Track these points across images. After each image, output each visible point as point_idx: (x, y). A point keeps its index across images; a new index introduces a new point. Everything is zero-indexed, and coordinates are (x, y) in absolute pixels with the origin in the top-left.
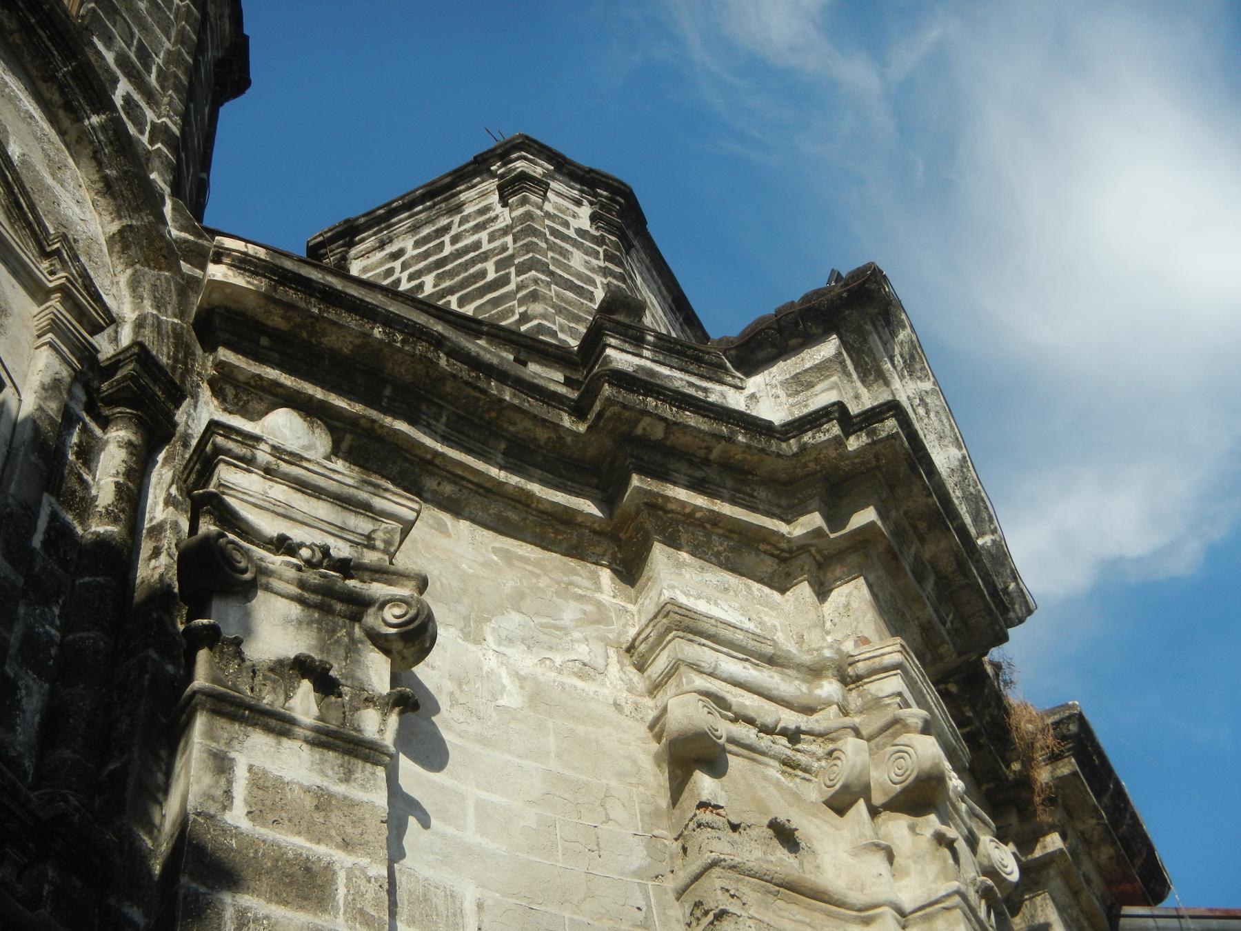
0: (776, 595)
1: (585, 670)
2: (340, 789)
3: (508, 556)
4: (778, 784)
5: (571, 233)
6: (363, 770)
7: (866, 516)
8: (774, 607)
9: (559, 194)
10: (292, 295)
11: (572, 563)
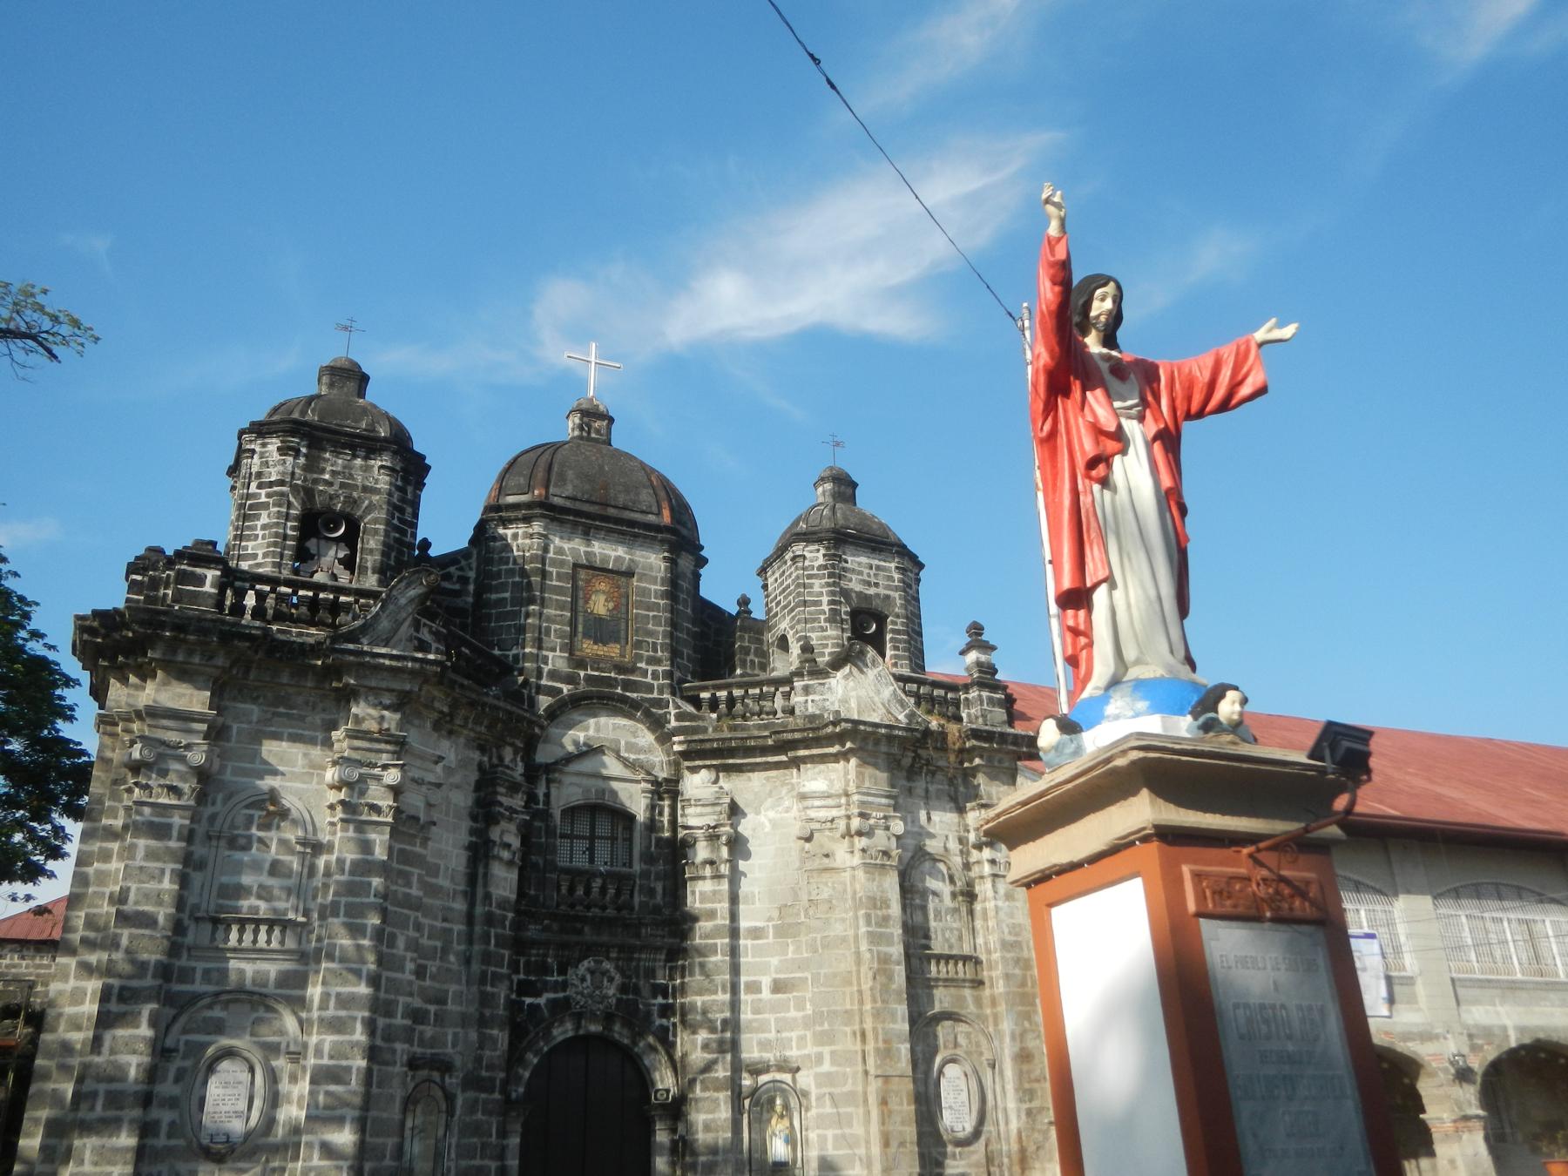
0: (837, 765)
2: (717, 888)
3: (767, 779)
4: (828, 837)
5: (815, 572)
6: (722, 880)
7: (849, 745)
8: (834, 770)
9: (811, 552)
10: (693, 745)
11: (786, 771)
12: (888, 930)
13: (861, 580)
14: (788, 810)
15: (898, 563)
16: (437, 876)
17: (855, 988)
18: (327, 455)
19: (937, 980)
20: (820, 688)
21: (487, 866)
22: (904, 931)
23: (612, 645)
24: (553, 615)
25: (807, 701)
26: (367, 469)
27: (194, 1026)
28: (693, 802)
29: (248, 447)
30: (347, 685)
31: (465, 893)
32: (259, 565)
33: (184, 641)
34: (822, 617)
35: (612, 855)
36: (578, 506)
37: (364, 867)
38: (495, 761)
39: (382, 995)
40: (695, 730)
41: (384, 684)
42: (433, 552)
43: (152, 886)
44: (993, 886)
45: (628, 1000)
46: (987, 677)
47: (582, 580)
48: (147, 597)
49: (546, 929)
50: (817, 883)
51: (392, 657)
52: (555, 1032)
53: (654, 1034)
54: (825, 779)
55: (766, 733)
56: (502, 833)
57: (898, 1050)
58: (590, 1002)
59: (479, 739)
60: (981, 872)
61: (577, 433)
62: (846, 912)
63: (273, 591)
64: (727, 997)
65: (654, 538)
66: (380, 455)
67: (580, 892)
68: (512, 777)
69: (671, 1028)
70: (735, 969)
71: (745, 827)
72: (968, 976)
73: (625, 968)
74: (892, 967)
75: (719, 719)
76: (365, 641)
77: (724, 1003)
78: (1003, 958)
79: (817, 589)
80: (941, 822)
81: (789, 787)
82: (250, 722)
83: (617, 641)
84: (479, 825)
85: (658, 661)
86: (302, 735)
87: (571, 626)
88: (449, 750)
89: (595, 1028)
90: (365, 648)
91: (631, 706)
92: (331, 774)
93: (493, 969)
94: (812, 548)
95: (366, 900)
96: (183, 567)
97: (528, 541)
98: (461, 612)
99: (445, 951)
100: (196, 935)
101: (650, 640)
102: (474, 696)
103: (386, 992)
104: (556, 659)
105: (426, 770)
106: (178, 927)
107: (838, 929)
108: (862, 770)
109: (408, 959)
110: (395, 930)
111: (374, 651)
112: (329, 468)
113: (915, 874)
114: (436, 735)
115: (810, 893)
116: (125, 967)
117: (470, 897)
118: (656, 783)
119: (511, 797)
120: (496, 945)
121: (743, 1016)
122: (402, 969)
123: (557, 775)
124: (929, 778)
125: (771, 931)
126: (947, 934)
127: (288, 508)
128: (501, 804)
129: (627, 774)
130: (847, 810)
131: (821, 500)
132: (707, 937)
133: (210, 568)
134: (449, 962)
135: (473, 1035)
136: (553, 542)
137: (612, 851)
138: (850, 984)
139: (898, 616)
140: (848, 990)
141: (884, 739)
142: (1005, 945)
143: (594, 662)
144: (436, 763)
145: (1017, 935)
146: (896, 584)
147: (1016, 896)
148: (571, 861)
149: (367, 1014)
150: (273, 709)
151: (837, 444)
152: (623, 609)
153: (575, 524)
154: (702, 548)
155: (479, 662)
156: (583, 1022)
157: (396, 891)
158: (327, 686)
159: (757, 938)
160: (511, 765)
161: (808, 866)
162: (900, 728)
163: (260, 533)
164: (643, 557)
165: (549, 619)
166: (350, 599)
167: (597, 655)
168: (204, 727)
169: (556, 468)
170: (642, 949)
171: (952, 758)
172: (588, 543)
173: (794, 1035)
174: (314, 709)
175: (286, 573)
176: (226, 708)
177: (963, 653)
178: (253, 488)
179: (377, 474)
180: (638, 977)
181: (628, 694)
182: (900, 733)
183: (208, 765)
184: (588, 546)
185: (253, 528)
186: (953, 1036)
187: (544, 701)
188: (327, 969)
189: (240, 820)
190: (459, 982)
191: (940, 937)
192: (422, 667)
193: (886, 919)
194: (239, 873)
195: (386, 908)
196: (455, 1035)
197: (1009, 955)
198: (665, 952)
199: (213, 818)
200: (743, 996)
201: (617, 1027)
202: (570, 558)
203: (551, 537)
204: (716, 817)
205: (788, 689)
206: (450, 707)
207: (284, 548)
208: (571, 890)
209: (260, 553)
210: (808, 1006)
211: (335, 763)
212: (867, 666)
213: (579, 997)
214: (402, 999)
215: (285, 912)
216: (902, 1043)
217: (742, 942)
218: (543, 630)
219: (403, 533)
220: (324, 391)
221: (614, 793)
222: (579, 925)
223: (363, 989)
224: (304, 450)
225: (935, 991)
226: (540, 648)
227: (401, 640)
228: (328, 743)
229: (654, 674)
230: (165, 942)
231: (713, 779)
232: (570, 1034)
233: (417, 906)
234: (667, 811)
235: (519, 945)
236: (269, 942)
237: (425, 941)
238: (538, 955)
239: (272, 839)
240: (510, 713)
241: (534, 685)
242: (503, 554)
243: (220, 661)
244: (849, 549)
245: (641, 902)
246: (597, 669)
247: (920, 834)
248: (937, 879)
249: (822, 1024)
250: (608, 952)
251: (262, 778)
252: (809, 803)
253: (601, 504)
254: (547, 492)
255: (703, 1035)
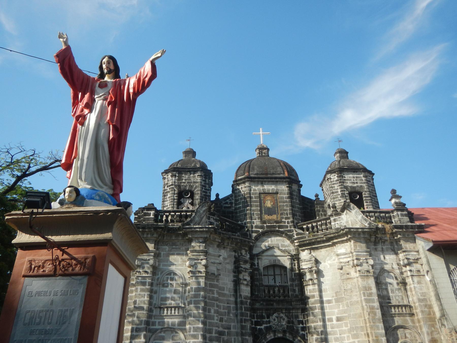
1: (334, 260)
2: (314, 288)
3: (327, 251)
4: (348, 268)
5: (335, 182)
8: (347, 245)
9: (333, 176)
10: (301, 243)
11: (332, 247)
12: (372, 298)
13: (351, 182)
14: (334, 260)
15: (364, 174)
16: (224, 290)
17: (363, 319)
18: (183, 175)
19: (395, 314)
20: (339, 219)
21: (239, 286)
22: (378, 298)
23: (274, 215)
24: (255, 209)
25: (335, 224)
26: (194, 177)
27: (156, 338)
28: (303, 261)
29: (164, 177)
30: (189, 238)
31: (234, 295)
32: (168, 208)
33: (146, 231)
34: (339, 196)
35: (281, 280)
36: (259, 176)
37: (198, 290)
38: (240, 254)
39: (208, 327)
40: (302, 238)
41: (199, 236)
42: (221, 197)
43: (142, 299)
44: (412, 279)
45: (290, 326)
46: (401, 207)
47: (262, 197)
48: (138, 221)
49: (261, 305)
50: (346, 283)
51: (200, 228)
52: (268, 337)
53: (300, 337)
54: (345, 249)
55: (323, 236)
56: (243, 276)
57: (381, 340)
58: (277, 327)
59: (233, 248)
60: (407, 275)
61: (258, 155)
62: (357, 292)
63: (170, 214)
64: (321, 323)
65: (283, 181)
66: (197, 172)
67: (271, 292)
68: (245, 259)
69: (306, 334)
70: (323, 314)
71: (321, 267)
72: (407, 312)
73: (288, 315)
74: (375, 310)
75: (309, 233)
76: (192, 224)
77: (321, 326)
78: (419, 305)
79: (336, 188)
80: (389, 259)
81: (334, 252)
82: (166, 251)
83: (275, 214)
84: (236, 274)
85: (289, 218)
86: (180, 253)
87: (260, 211)
88: (224, 253)
89: (280, 335)
90: (192, 227)
91: (281, 233)
92: (188, 263)
93: (244, 318)
94: (333, 175)
95: (199, 299)
96: (145, 212)
97: (245, 189)
98: (232, 213)
99: (229, 313)
100: (156, 312)
101: (285, 212)
102: (227, 236)
103: (209, 326)
104: (257, 222)
105: (216, 259)
106: (150, 310)
107: (355, 299)
108: (356, 244)
109: (215, 316)
110: (210, 308)
111: (195, 227)
112: (184, 179)
113: (382, 278)
114: (218, 249)
115: (344, 287)
116: (138, 322)
117: (236, 296)
118: (292, 256)
119: (245, 265)
120: (245, 310)
121: (328, 330)
122: (214, 319)
123: (260, 257)
124: (382, 244)
125: (334, 301)
126: (397, 298)
127: (174, 191)
128: (242, 267)
129: (282, 254)
130: (352, 258)
131: (336, 159)
132: (313, 304)
133: (151, 211)
134: (231, 317)
135: (240, 339)
136: (252, 188)
137: (281, 279)
138: (362, 317)
139: (366, 192)
140: (361, 319)
141: (362, 233)
142: (420, 300)
143: (269, 221)
144: (219, 257)
145: (424, 296)
146: (364, 181)
147: (422, 282)
148: (269, 283)
149: (202, 333)
150: (171, 247)
151: (340, 141)
152: (276, 204)
153: (258, 181)
154: (300, 181)
155: (233, 226)
156: (276, 333)
157: (209, 296)
158: (185, 239)
159: (329, 303)
160: (245, 255)
161: (342, 278)
162: (366, 229)
163: (168, 199)
164: (280, 187)
165: (254, 211)
166: (190, 213)
167: (269, 219)
168: (153, 254)
169: (251, 166)
170: (293, 309)
171: (388, 236)
172: (263, 186)
173: (345, 335)
174: (182, 245)
175: (175, 209)
176: (160, 248)
177: (390, 200)
178: (166, 188)
179: (197, 178)
180: (293, 318)
181: (280, 230)
182: (367, 230)
183: (154, 264)
184: (263, 187)
185: (167, 198)
186: (404, 334)
187: (254, 235)
188: (190, 320)
189: (165, 279)
190: (234, 322)
191: (394, 299)
192: (208, 230)
193: (371, 294)
194: (166, 294)
195: (206, 301)
196: (235, 339)
197: (422, 304)
198: (300, 310)
199: (158, 279)
200: (327, 323)
201: (288, 335)
202: (258, 192)
203: (252, 186)
204: (311, 265)
205: (329, 221)
206: (221, 240)
207: (174, 202)
208: (269, 292)
209: (168, 205)
210: (349, 325)
211: (188, 260)
212: (351, 209)
213: (274, 325)
214: (214, 328)
215: (179, 304)
216: (383, 337)
217: (325, 305)
218: (252, 214)
219: (206, 193)
220: (184, 158)
221: (279, 261)
222: (272, 303)
223: (201, 325)
224: (177, 175)
225: (395, 318)
226: (251, 219)
227: (203, 223)
228: (187, 255)
229: (288, 222)
230: (147, 315)
231: (309, 253)
232: (273, 337)
233: (217, 300)
234: (296, 264)
235: (253, 310)
236: (175, 313)
237: (222, 310)
238: (260, 313)
239: (174, 283)
240: (241, 240)
241: (251, 231)
242: (239, 194)
243: (155, 235)
244: (345, 173)
245: (291, 294)
246: (270, 223)
247: (382, 264)
248: (390, 279)
249: (354, 332)
250: (282, 311)
251: (170, 267)
252: (340, 257)
253: (266, 174)
254: (249, 173)
255: (315, 336)
